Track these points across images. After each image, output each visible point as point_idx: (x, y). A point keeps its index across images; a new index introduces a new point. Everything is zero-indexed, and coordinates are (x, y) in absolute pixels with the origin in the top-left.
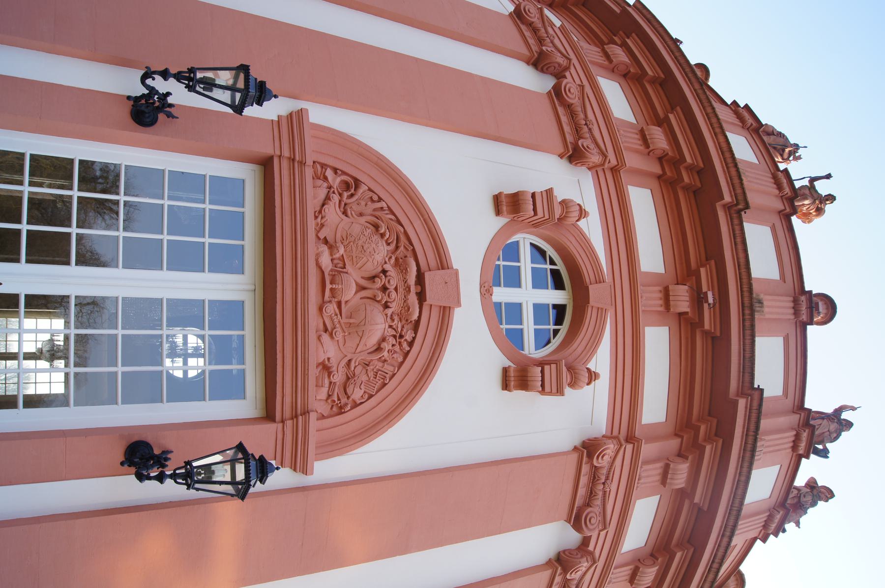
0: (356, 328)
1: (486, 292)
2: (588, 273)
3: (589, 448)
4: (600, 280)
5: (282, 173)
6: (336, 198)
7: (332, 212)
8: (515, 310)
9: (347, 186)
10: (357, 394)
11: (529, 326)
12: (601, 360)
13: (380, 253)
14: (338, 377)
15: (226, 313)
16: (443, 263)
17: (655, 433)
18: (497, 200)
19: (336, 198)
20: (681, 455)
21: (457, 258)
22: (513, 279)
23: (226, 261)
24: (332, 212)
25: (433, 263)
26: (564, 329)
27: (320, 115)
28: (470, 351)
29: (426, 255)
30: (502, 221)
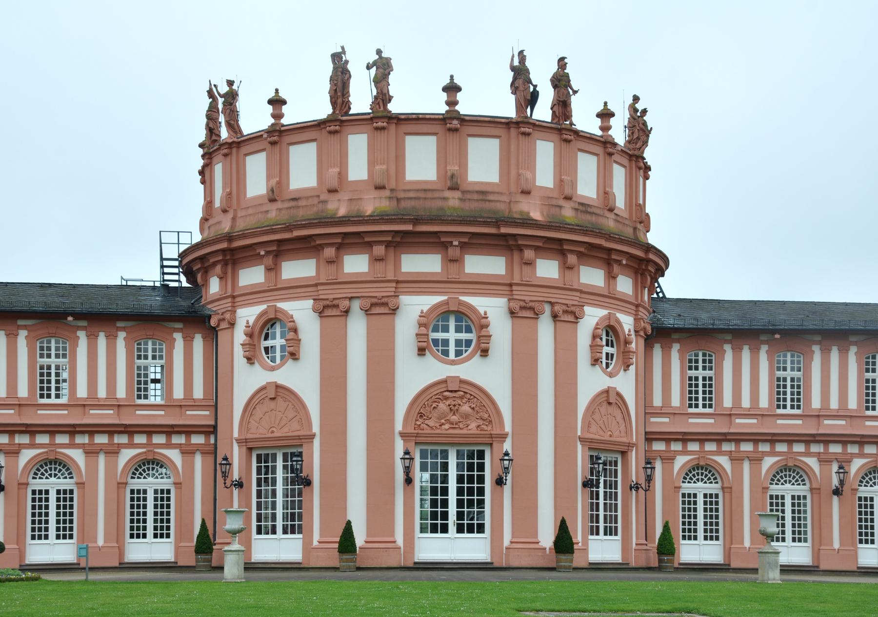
0: (466, 416)
1: (453, 363)
2: (444, 309)
3: (512, 313)
4: (446, 303)
6: (426, 422)
7: (431, 423)
8: (458, 343)
9: (421, 416)
10: (486, 416)
11: (464, 336)
12: (480, 303)
13: (443, 406)
14: (481, 422)
15: (459, 455)
16: (444, 382)
17: (510, 267)
18: (419, 355)
19: (426, 422)
20: (521, 250)
22: (446, 342)
24: (431, 423)
25: (444, 385)
26: (465, 318)
27: (399, 426)
28: (473, 370)
29: (442, 388)
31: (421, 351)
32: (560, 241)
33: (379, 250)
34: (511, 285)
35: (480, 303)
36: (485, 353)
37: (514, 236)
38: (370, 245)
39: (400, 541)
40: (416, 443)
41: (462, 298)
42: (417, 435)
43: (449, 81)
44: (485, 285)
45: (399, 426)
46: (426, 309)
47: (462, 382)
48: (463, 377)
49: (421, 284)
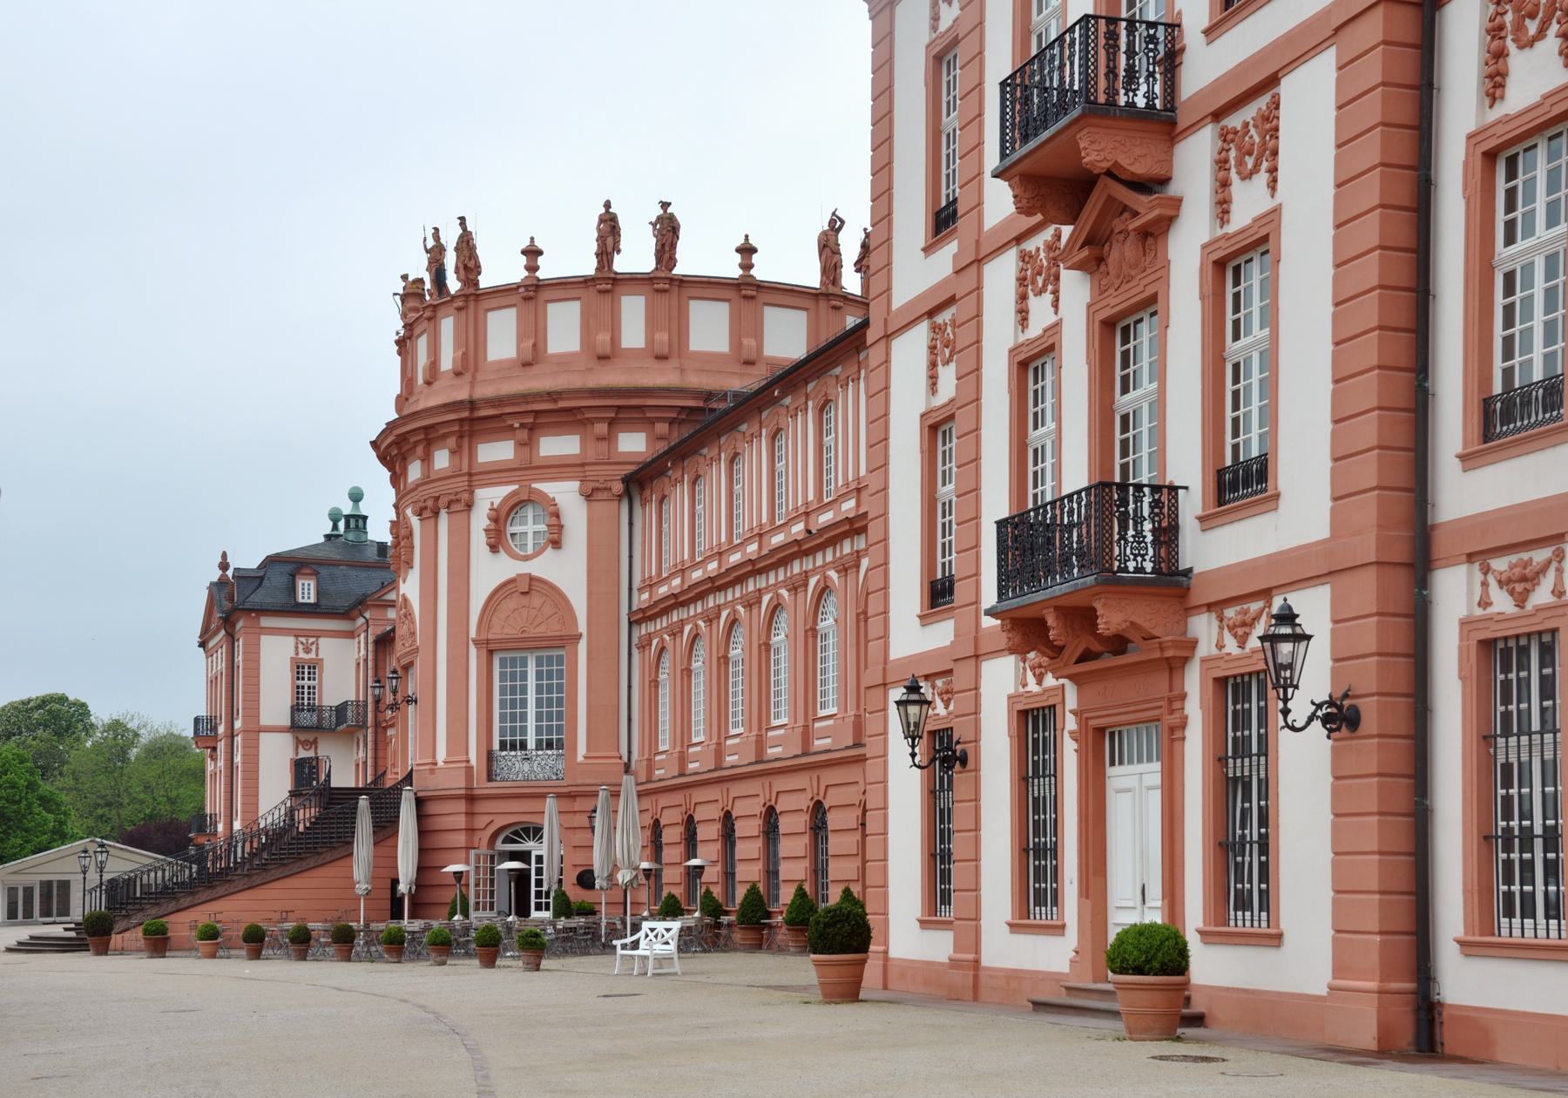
1: (526, 558)
5: (492, 646)
12: (548, 488)
15: (539, 663)
21: (512, 575)
23: (524, 663)
27: (473, 634)
28: (546, 566)
30: (502, 551)
31: (494, 548)
32: (640, 407)
33: (452, 441)
34: (583, 465)
35: (548, 488)
36: (556, 544)
37: (579, 408)
38: (445, 436)
39: (473, 762)
40: (491, 652)
41: (534, 485)
42: (488, 641)
43: (528, 243)
44: (559, 469)
45: (473, 634)
46: (497, 502)
47: (532, 579)
48: (536, 573)
49: (497, 473)
